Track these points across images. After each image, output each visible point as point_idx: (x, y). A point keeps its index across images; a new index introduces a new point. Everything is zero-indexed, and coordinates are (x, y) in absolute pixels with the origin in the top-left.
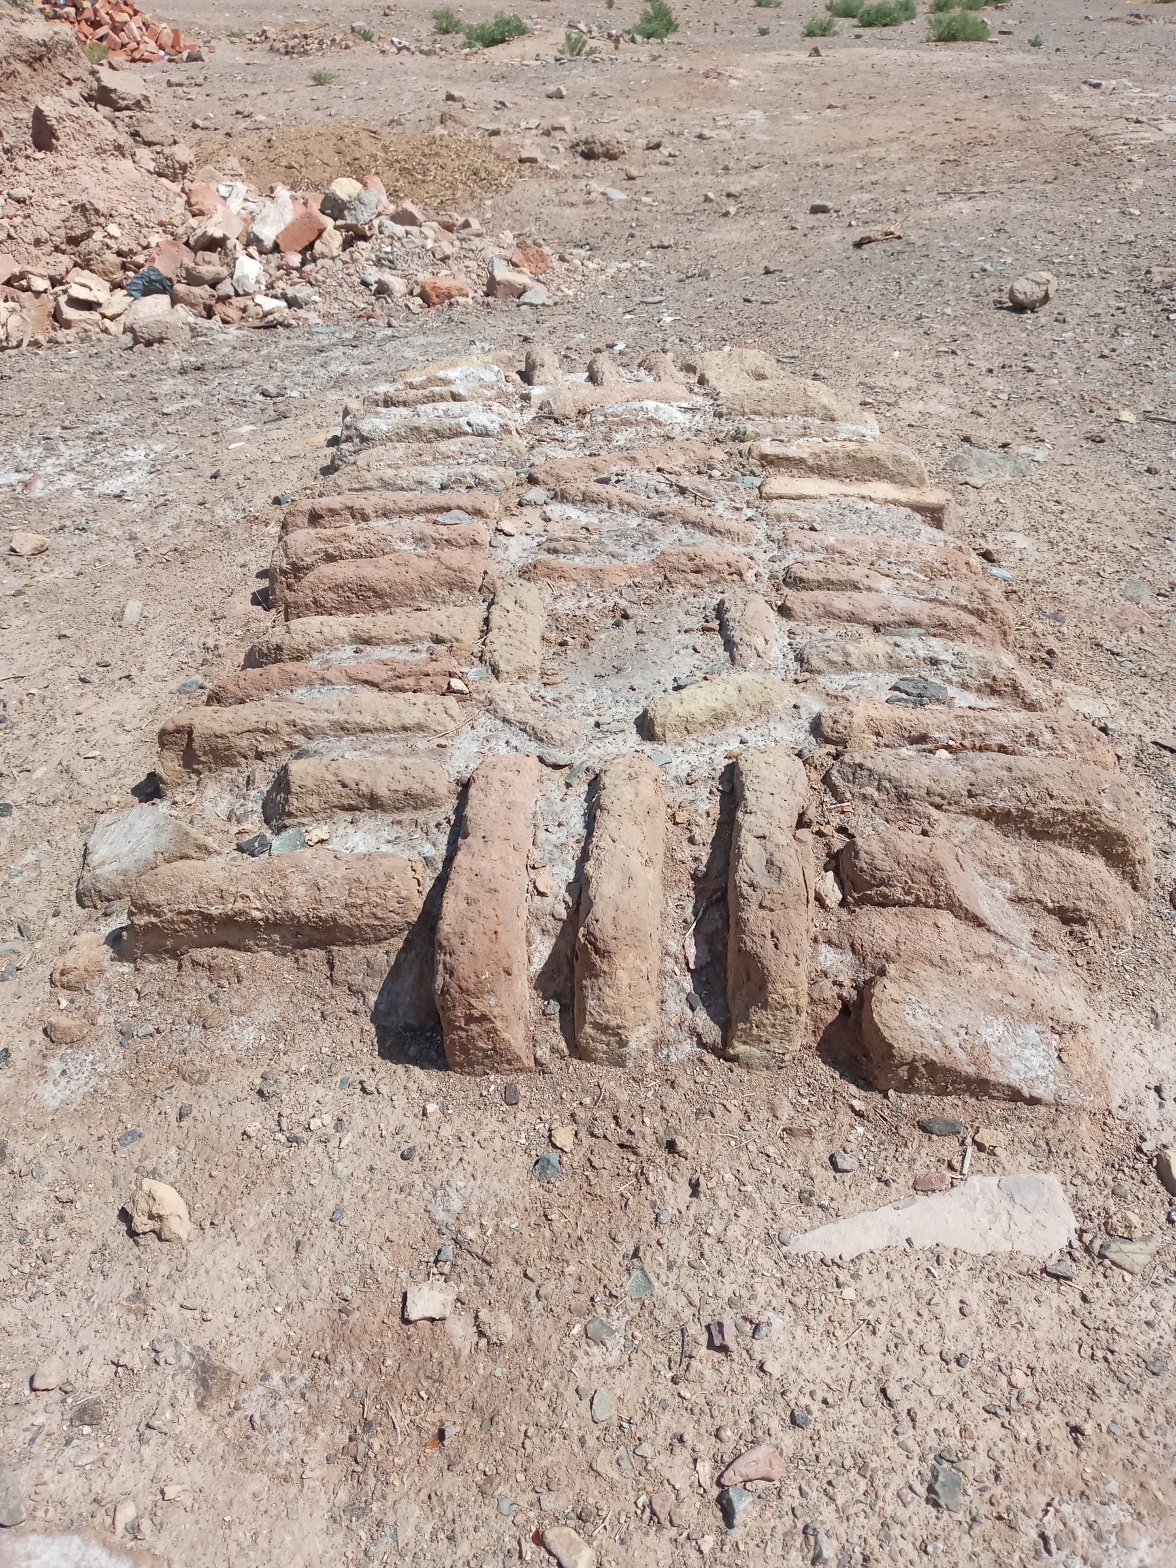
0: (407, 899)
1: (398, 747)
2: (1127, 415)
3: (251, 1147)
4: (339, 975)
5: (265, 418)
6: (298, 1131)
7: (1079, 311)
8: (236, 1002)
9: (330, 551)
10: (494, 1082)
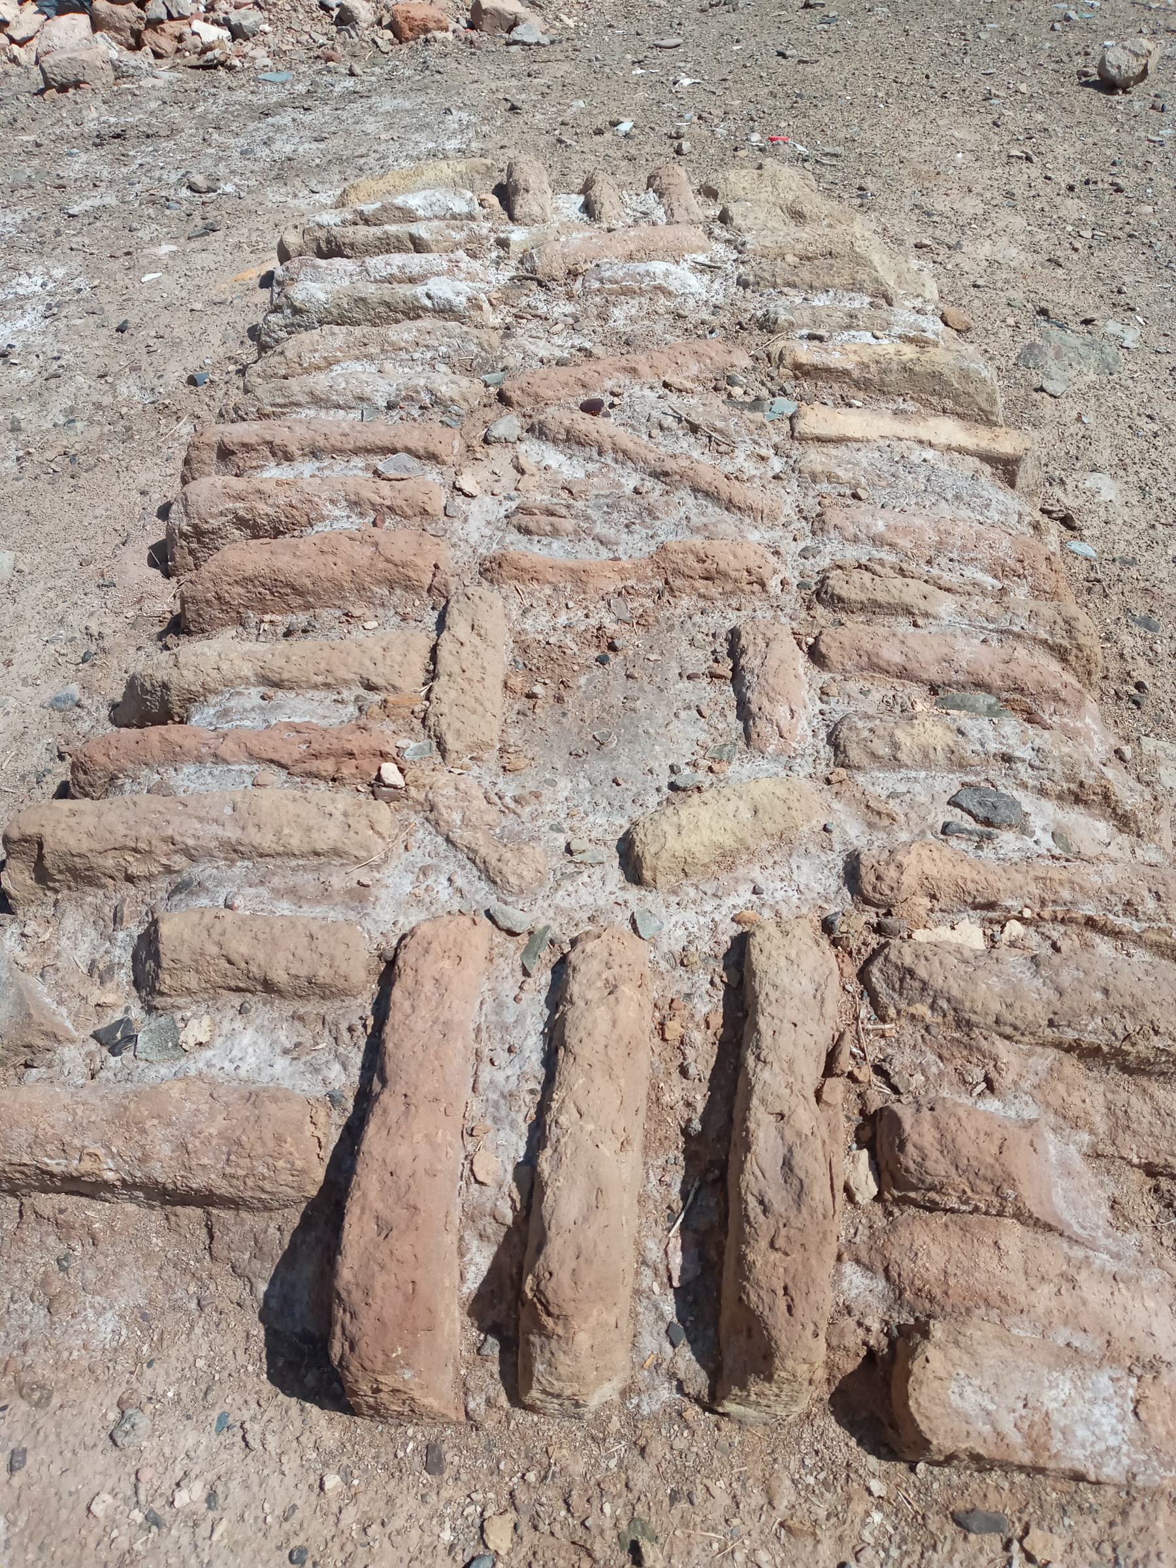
0: (303, 1171)
1: (307, 881)
3: (98, 1531)
5: (190, 229)
6: (158, 1505)
9: (241, 513)
10: (415, 1436)
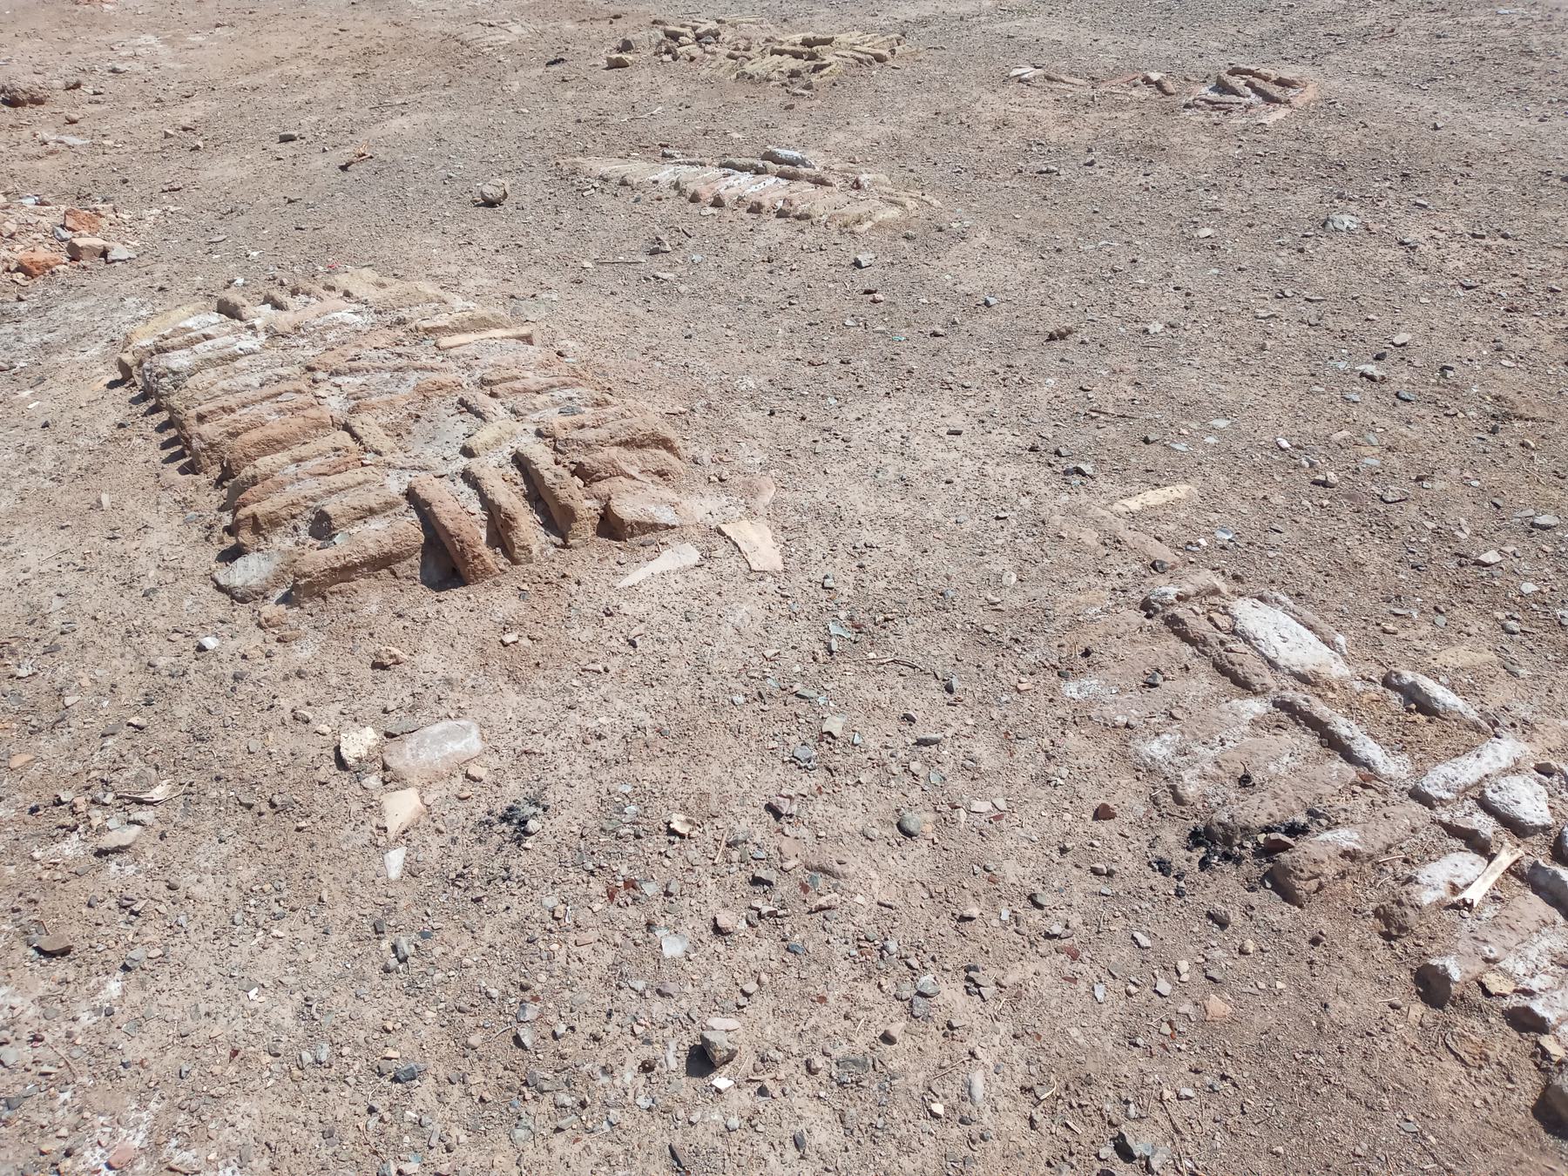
2: (586, 264)
7: (528, 199)
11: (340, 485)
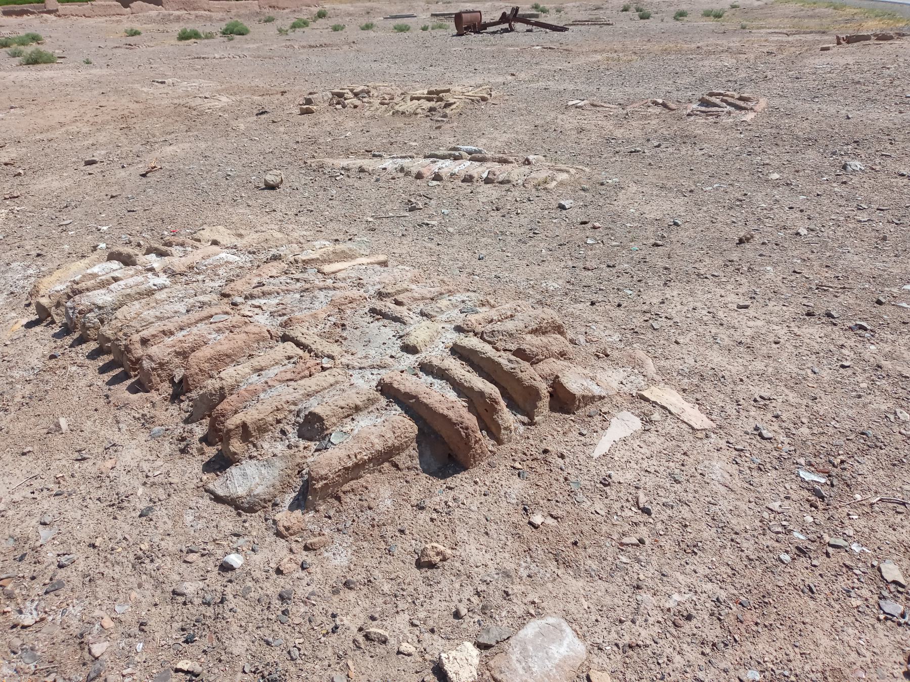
4: (401, 466)
8: (373, 496)
11: (314, 388)
